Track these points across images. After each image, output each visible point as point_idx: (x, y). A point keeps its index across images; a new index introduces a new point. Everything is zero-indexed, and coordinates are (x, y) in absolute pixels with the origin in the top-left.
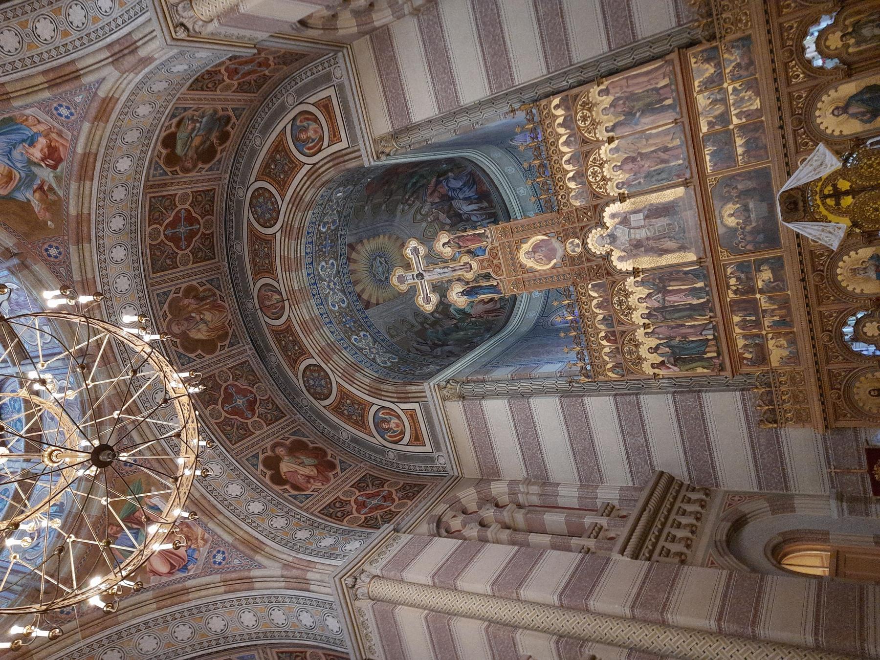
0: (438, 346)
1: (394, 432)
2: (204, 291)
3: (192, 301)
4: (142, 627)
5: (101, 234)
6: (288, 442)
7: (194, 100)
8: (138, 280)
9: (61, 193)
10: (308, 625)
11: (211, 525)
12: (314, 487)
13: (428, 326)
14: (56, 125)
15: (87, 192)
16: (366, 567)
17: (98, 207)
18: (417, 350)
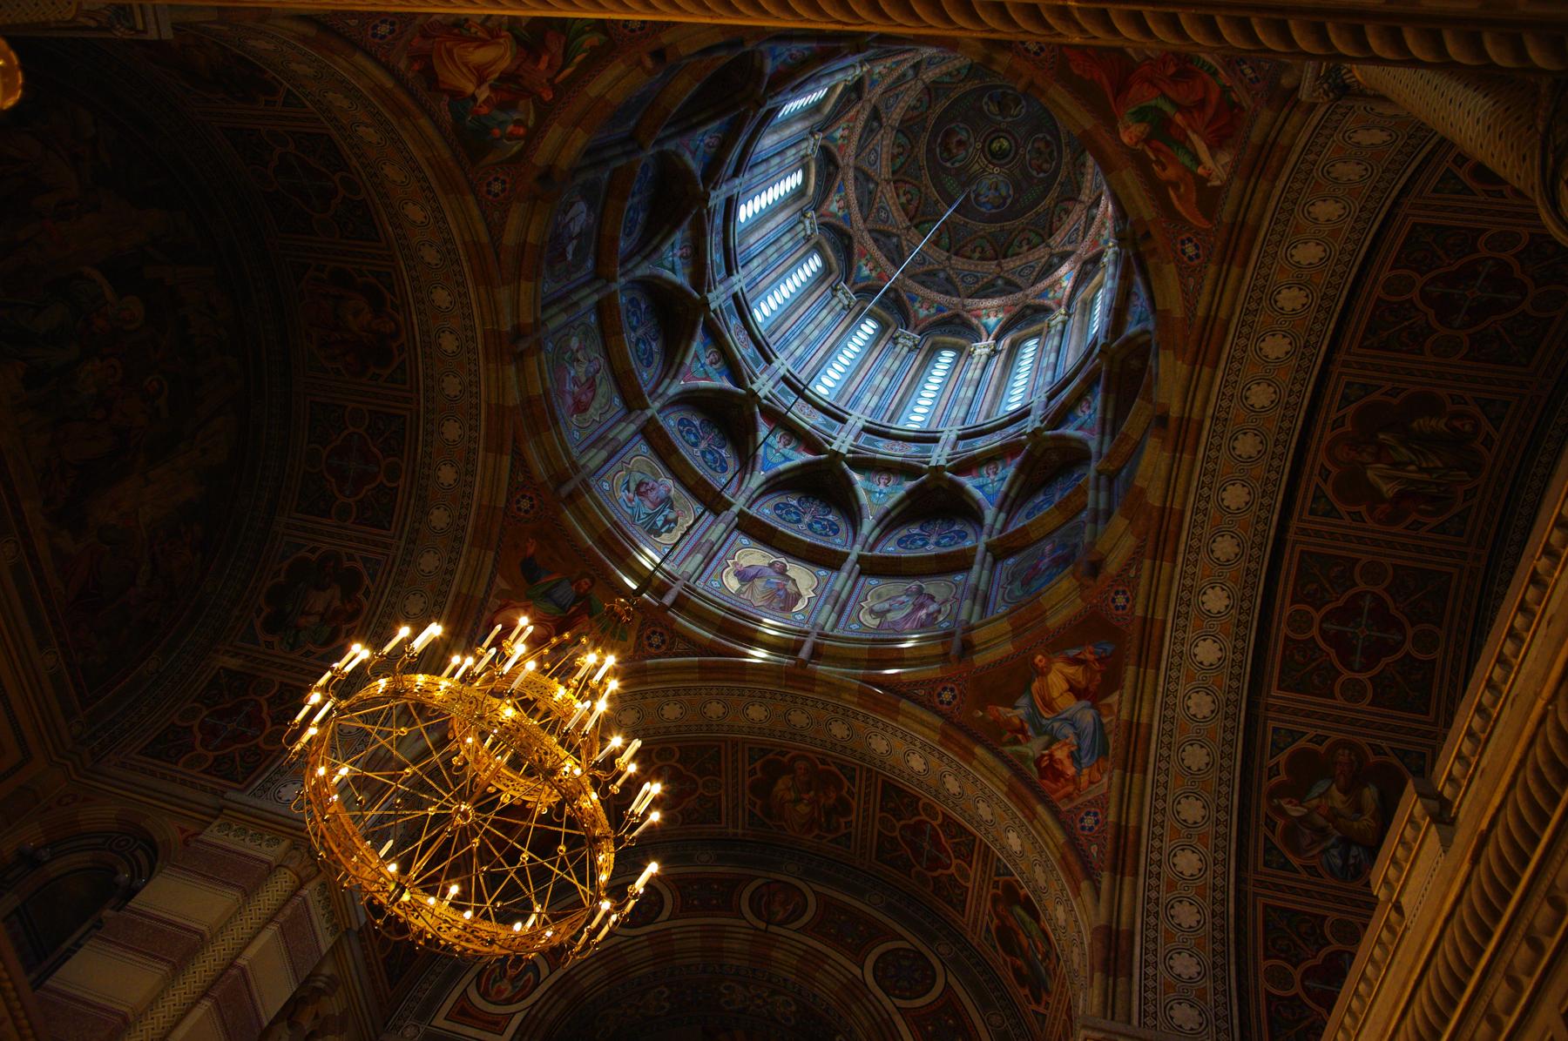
1: (495, 981)
3: (831, 801)
9: (1007, 749)
14: (1080, 800)
17: (976, 780)
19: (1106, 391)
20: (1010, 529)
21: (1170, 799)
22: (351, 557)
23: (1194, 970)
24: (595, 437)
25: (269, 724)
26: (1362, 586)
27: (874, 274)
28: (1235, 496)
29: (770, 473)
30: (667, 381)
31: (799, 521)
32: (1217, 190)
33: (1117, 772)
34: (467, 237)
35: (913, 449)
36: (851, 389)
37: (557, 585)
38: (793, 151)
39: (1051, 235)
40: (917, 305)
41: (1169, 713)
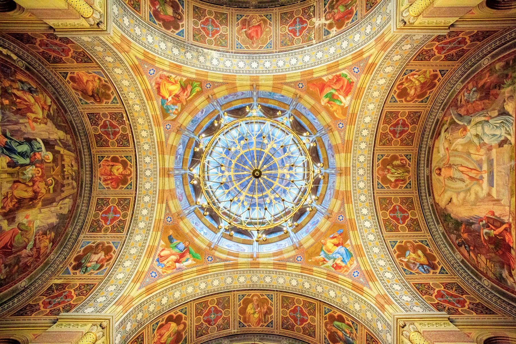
2: (268, 318)
3: (265, 310)
4: (146, 238)
5: (303, 277)
6: (183, 333)
7: (361, 334)
8: (281, 287)
9: (322, 266)
11: (169, 277)
12: (156, 336)
15: (322, 276)
21: (375, 261)
23: (409, 299)
26: (395, 204)
28: (362, 185)
32: (347, 107)
33: (358, 258)
34: (159, 140)
37: (179, 244)
41: (364, 241)
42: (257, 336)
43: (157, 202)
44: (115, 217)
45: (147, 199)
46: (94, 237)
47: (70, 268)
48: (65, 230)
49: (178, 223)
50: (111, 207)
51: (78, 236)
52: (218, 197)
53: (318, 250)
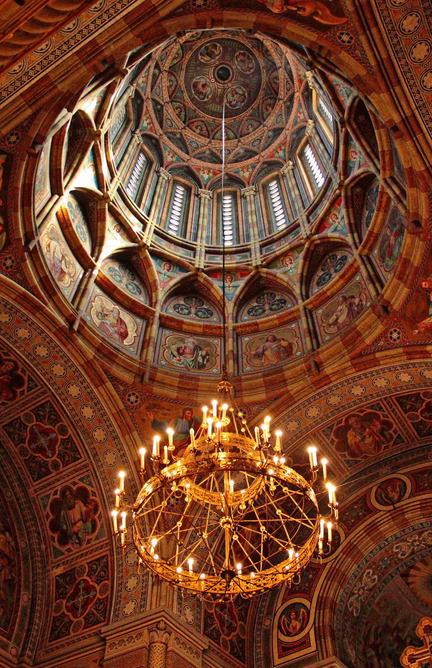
0: (377, 651)
2: (390, 434)
3: (379, 427)
10: (128, 585)
13: (395, 634)
16: (173, 635)
18: (369, 631)
19: (358, 139)
20: (364, 239)
22: (75, 484)
24: (141, 344)
25: (96, 585)
27: (211, 174)
29: (234, 299)
30: (154, 294)
31: (264, 311)
35: (291, 237)
36: (241, 233)
38: (131, 147)
39: (277, 94)
40: (241, 173)
42: (385, 464)
43: (93, 387)
44: (51, 440)
45: (74, 390)
46: (49, 484)
47: (57, 545)
48: (5, 502)
49: (150, 391)
50: (32, 428)
51: (26, 495)
52: (179, 238)
53: (423, 305)
